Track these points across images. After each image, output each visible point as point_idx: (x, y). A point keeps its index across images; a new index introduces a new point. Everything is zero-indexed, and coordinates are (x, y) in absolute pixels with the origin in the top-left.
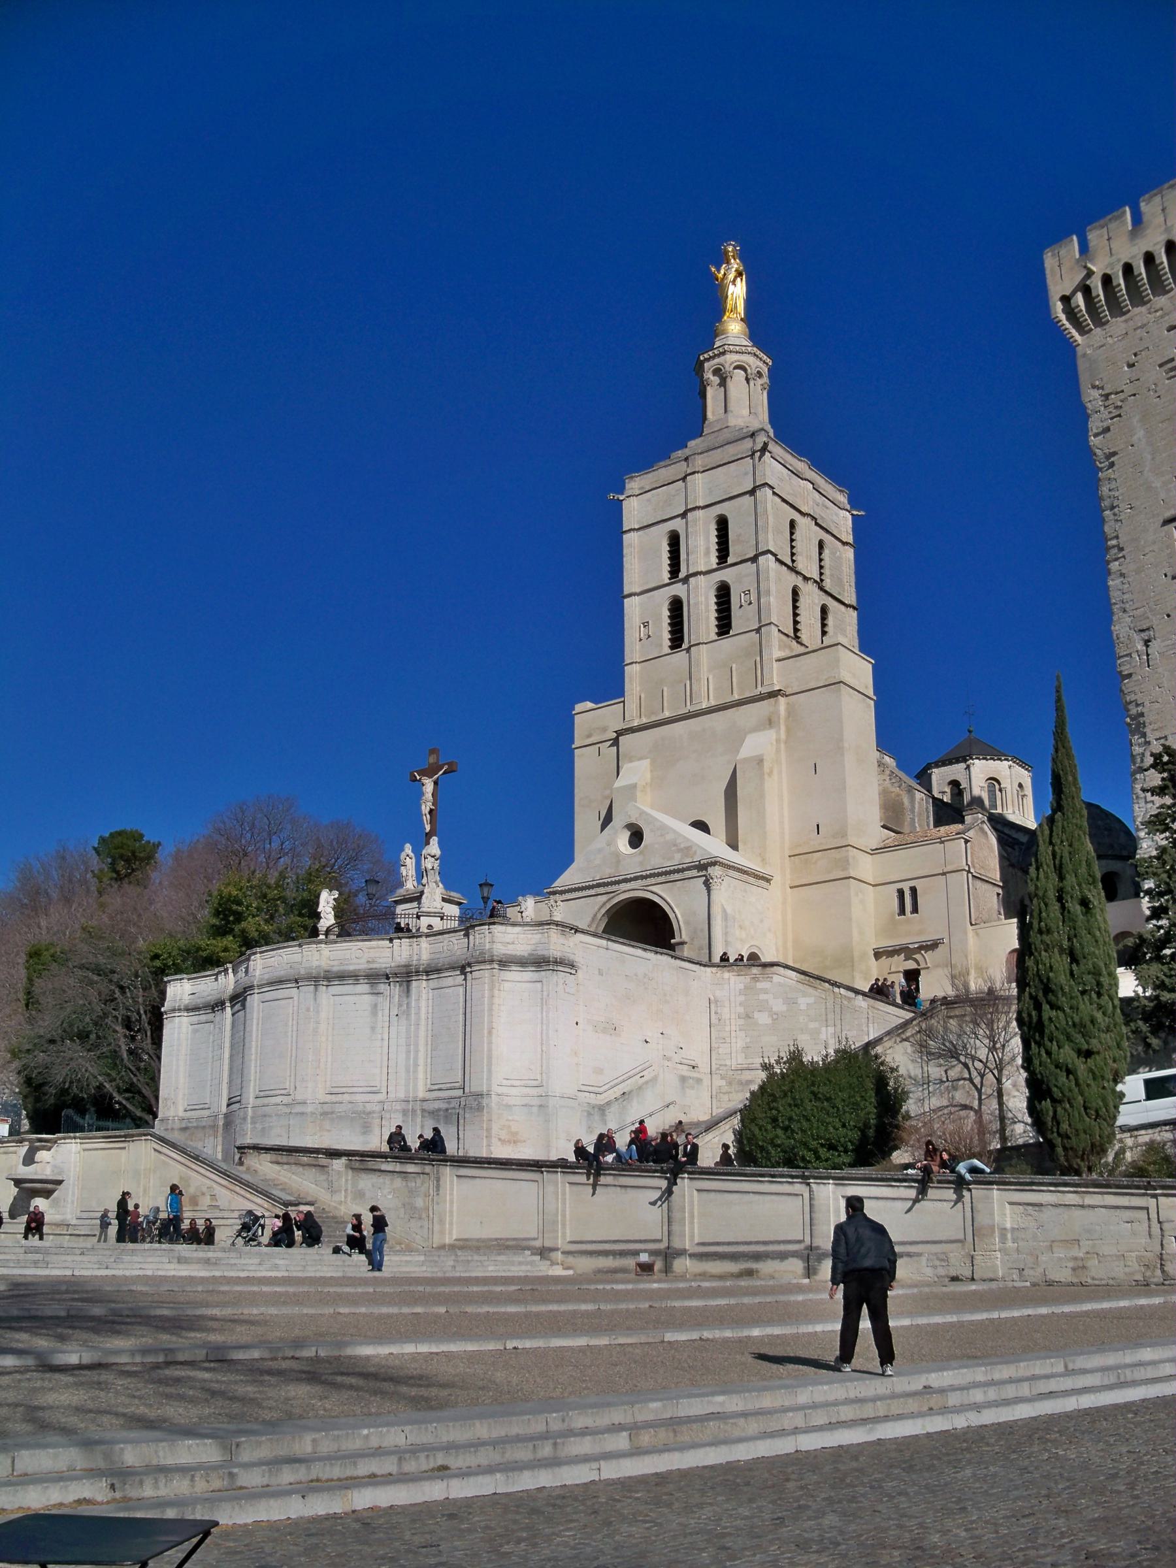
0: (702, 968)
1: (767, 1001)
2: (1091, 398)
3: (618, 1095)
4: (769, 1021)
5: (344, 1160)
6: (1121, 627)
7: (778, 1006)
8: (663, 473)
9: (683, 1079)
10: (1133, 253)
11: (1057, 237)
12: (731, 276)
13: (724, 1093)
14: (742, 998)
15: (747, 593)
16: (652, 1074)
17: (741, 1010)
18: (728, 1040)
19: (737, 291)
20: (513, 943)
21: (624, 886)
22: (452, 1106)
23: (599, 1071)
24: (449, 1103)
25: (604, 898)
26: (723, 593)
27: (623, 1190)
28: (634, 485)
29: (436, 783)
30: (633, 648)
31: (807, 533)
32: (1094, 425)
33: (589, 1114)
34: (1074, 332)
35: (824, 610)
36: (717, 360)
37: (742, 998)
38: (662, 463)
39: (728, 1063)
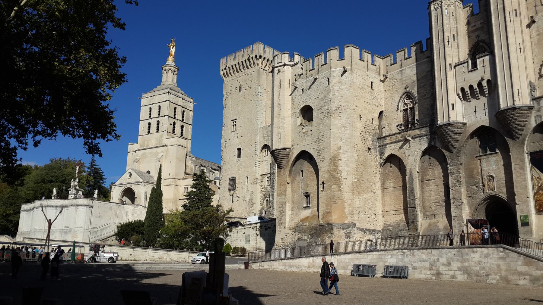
2: (224, 92)
5: (39, 240)
6: (223, 141)
7: (139, 213)
8: (150, 94)
10: (233, 63)
11: (223, 57)
12: (172, 47)
15: (162, 123)
19: (173, 50)
21: (127, 185)
23: (97, 225)
25: (123, 187)
26: (158, 122)
28: (144, 96)
29: (79, 167)
30: (140, 133)
31: (179, 111)
32: (224, 98)
34: (224, 77)
35: (182, 126)
36: (165, 68)
38: (151, 91)
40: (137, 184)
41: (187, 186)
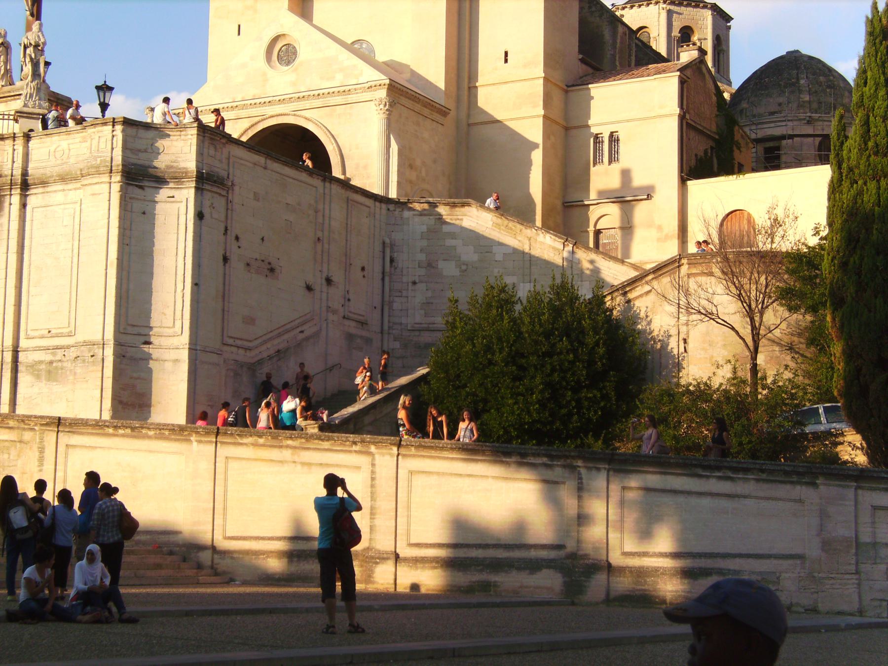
0: (377, 204)
1: (455, 248)
3: (272, 352)
4: (456, 272)
9: (350, 337)
13: (398, 358)
14: (425, 243)
16: (314, 329)
17: (422, 257)
18: (404, 293)
20: (146, 151)
22: (58, 357)
24: (54, 354)
27: (306, 468)
33: (236, 374)
37: (425, 243)
39: (404, 321)
40: (339, 100)
41: (613, 128)
